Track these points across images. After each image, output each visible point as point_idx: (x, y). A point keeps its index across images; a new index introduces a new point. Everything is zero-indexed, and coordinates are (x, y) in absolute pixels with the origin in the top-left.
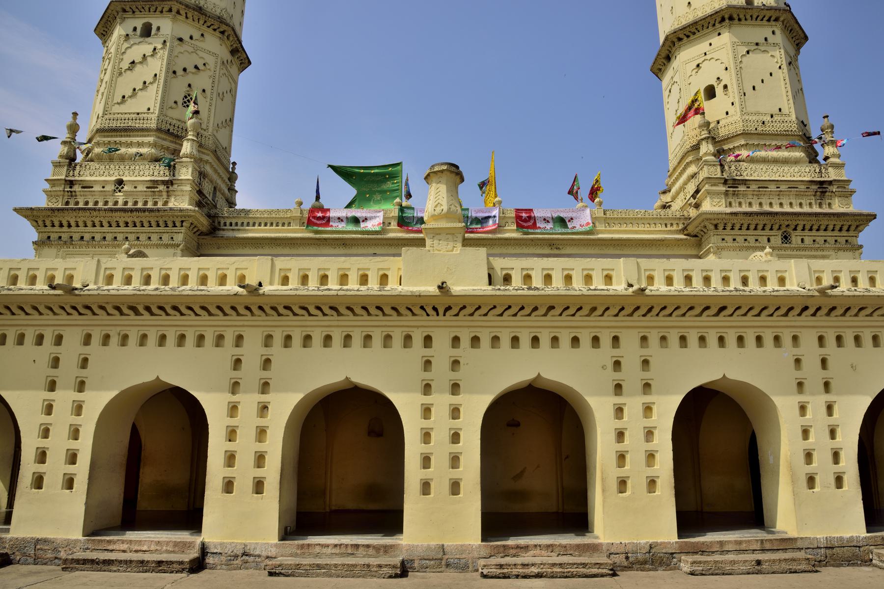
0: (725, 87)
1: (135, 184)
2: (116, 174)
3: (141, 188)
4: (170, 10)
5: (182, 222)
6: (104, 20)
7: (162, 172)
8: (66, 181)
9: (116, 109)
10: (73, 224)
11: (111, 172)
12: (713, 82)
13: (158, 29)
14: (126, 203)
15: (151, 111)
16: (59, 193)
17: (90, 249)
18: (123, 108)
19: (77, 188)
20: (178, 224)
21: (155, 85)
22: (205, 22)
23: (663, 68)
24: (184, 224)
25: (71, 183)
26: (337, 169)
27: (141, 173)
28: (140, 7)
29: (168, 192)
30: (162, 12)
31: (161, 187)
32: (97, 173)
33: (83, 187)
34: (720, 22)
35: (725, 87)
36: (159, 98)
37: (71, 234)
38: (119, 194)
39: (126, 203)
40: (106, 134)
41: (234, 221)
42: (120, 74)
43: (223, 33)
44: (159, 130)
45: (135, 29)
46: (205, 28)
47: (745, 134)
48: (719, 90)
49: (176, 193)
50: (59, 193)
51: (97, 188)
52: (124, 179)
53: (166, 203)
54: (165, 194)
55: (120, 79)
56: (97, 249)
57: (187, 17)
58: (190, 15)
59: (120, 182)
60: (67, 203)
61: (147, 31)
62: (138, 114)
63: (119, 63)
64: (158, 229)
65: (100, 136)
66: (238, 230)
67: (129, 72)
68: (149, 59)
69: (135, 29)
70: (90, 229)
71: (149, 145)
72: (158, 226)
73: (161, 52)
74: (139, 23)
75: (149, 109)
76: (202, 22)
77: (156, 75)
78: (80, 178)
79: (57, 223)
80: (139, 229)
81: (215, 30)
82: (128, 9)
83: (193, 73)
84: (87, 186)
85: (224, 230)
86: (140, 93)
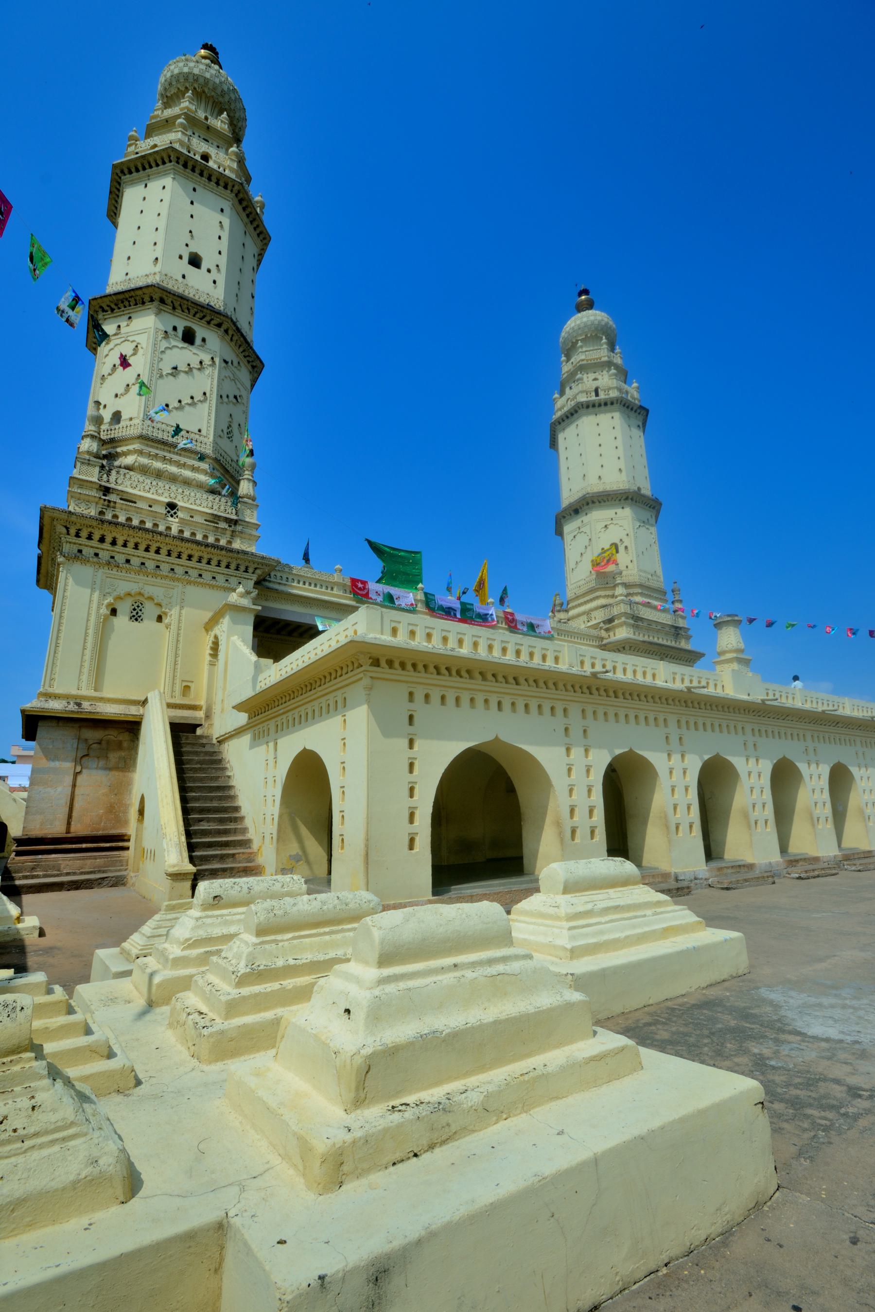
0: (626, 547)
1: (192, 513)
2: (166, 494)
3: (198, 519)
4: (219, 325)
5: (256, 569)
6: (121, 297)
7: (222, 508)
8: (101, 486)
10: (120, 542)
11: (160, 491)
12: (617, 541)
14: (181, 531)
15: (204, 432)
16: (93, 499)
17: (141, 577)
19: (112, 497)
20: (251, 570)
21: (206, 405)
22: (244, 351)
23: (567, 517)
24: (258, 572)
25: (107, 490)
26: (370, 543)
27: (198, 502)
28: (185, 307)
29: (233, 532)
31: (223, 525)
32: (141, 486)
33: (121, 499)
35: (626, 547)
37: (113, 554)
38: (170, 519)
39: (181, 531)
40: (150, 443)
41: (279, 574)
42: (161, 376)
43: (253, 367)
44: (216, 460)
46: (241, 356)
47: (641, 586)
49: (243, 535)
50: (91, 499)
51: (140, 504)
52: (180, 504)
53: (229, 542)
54: (229, 533)
55: (160, 382)
56: (150, 578)
57: (231, 340)
58: (235, 338)
59: (172, 506)
60: (102, 513)
61: (189, 337)
63: (159, 362)
64: (226, 571)
65: (140, 443)
66: (285, 585)
67: (171, 378)
68: (195, 371)
70: (141, 552)
71: (205, 473)
72: (228, 567)
73: (210, 369)
74: (181, 325)
75: (200, 431)
76: (241, 349)
77: (205, 394)
78: (120, 488)
79: (96, 536)
80: (203, 565)
81: (249, 362)
82: (169, 301)
83: (234, 404)
84: (129, 499)
85: (270, 581)
86: (187, 408)
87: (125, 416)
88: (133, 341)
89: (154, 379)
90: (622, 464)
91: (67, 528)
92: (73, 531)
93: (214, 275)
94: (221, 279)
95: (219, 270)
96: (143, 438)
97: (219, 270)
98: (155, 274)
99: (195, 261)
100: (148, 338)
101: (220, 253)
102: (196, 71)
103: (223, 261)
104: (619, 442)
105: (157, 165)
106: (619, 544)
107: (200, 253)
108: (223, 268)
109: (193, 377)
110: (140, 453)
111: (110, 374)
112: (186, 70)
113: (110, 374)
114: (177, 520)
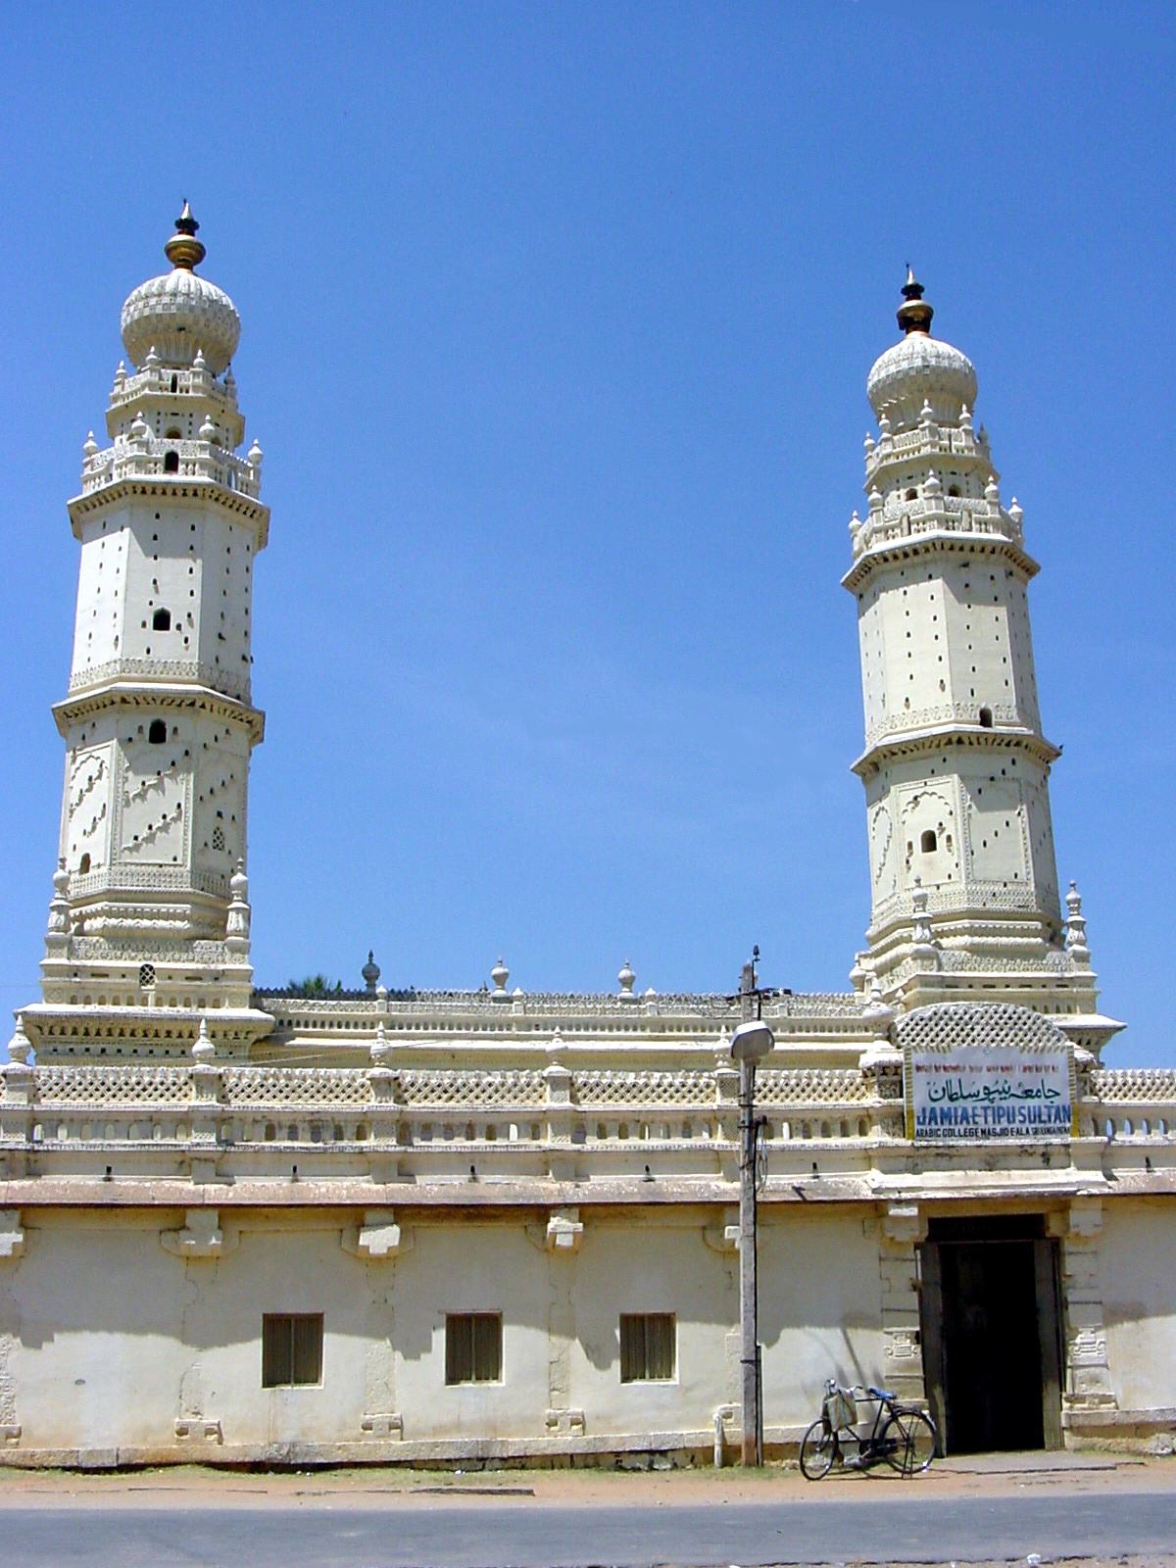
0: (949, 838)
9: (127, 857)
10: (93, 1032)
12: (935, 829)
13: (175, 730)
15: (179, 862)
18: (135, 858)
21: (181, 825)
30: (180, 705)
34: (946, 744)
35: (949, 838)
36: (190, 843)
38: (149, 987)
42: (128, 804)
45: (140, 729)
47: (972, 914)
48: (941, 842)
52: (156, 965)
62: (161, 866)
67: (138, 800)
68: (166, 780)
69: (140, 729)
71: (182, 917)
75: (175, 859)
77: (179, 806)
87: (93, 863)
88: (98, 758)
89: (119, 808)
90: (943, 671)
91: (41, 1029)
92: (46, 1030)
93: (187, 630)
94: (194, 635)
95: (191, 624)
96: (111, 895)
97: (191, 624)
98: (115, 662)
99: (162, 621)
100: (112, 754)
101: (192, 593)
102: (159, 310)
103: (195, 605)
104: (941, 626)
105: (114, 499)
106: (937, 833)
107: (166, 608)
108: (196, 618)
109: (164, 792)
110: (109, 914)
111: (77, 805)
112: (147, 312)
113: (77, 805)
114: (152, 987)
